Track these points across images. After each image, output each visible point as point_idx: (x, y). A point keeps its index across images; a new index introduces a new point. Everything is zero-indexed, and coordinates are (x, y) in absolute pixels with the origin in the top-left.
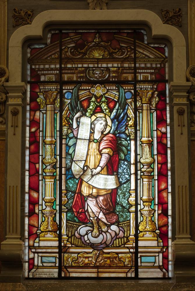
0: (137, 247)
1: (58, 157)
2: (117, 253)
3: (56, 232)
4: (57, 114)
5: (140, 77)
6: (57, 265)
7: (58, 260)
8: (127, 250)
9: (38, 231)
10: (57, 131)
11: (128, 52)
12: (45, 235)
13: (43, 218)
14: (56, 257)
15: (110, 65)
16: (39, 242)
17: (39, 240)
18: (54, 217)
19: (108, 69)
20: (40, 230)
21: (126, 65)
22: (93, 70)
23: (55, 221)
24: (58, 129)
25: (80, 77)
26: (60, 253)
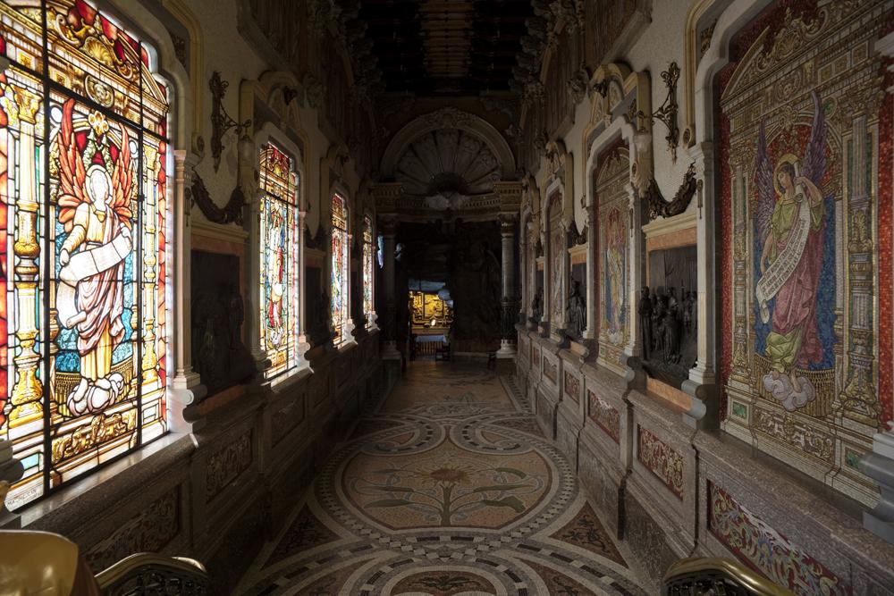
0: (139, 398)
1: (42, 242)
2: (120, 413)
3: (38, 400)
4: (39, 147)
5: (146, 123)
6: (42, 468)
7: (42, 456)
8: (130, 405)
9: (5, 409)
10: (40, 184)
11: (134, 73)
12: (21, 413)
13: (17, 374)
14: (39, 452)
15: (115, 85)
16: (8, 433)
17: (9, 428)
18: (36, 369)
19: (112, 89)
20: (10, 403)
21: (132, 95)
22: (95, 83)
23: (38, 379)
24: (43, 181)
25: (77, 86)
26: (47, 443)
